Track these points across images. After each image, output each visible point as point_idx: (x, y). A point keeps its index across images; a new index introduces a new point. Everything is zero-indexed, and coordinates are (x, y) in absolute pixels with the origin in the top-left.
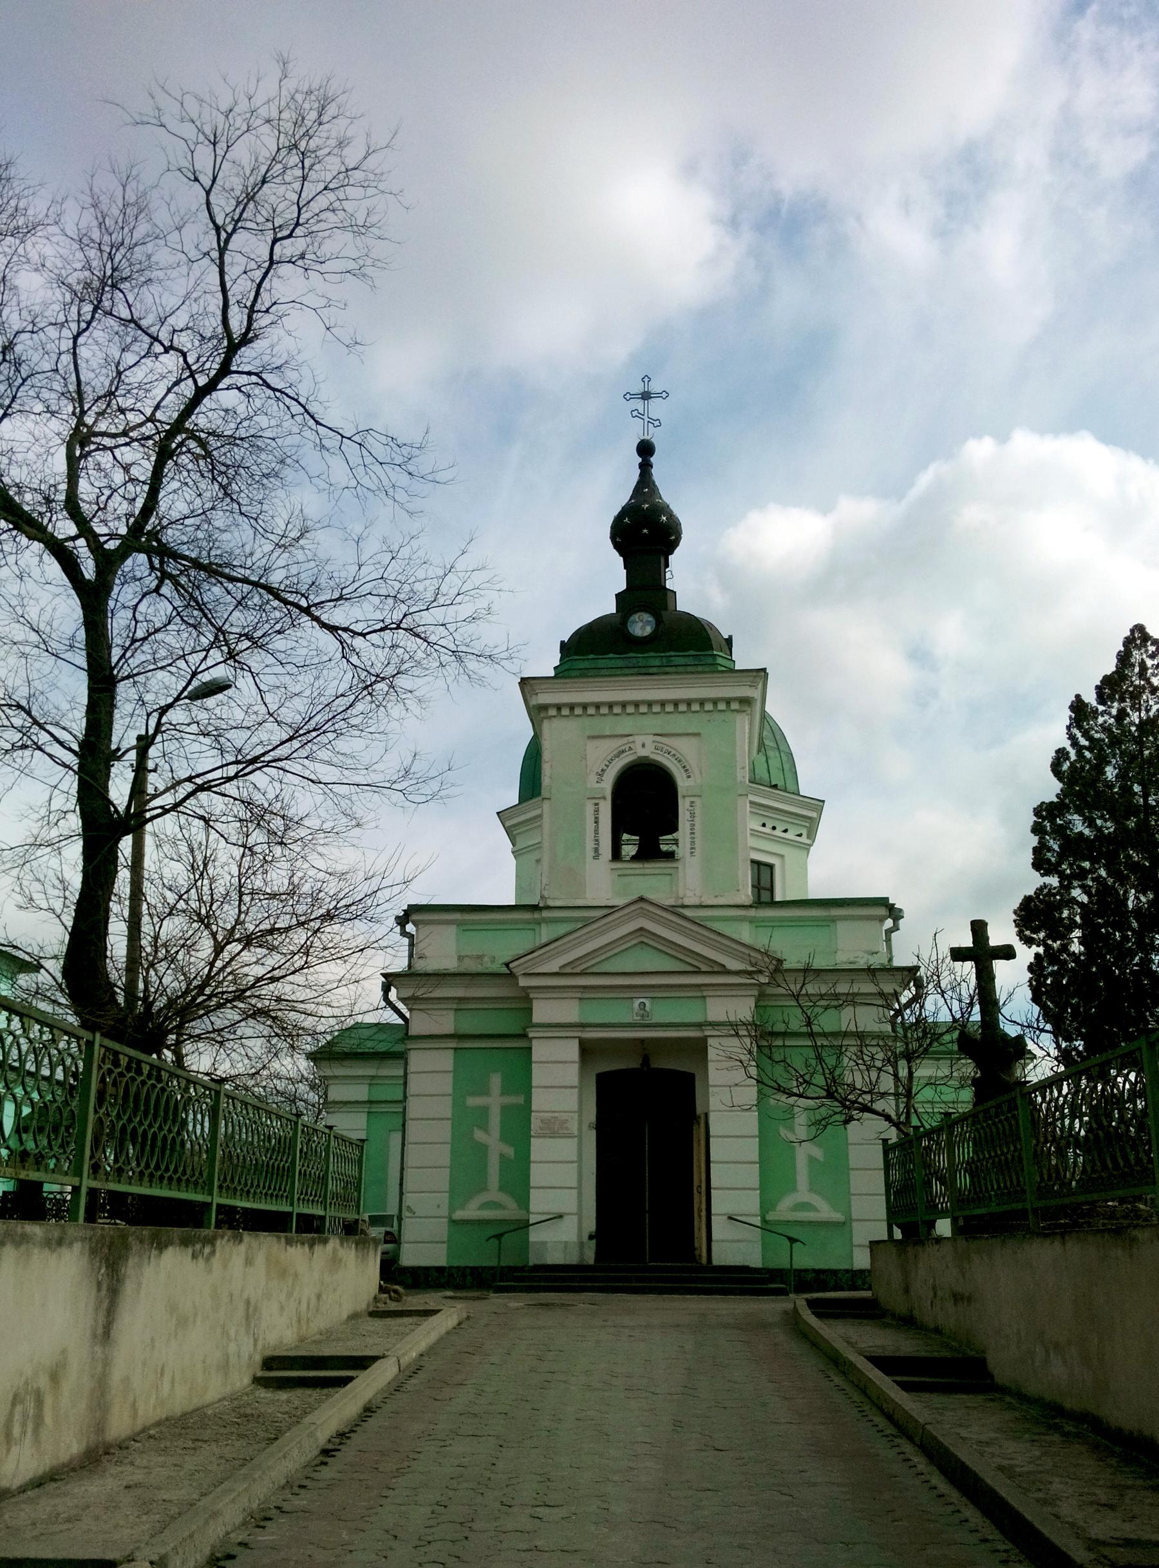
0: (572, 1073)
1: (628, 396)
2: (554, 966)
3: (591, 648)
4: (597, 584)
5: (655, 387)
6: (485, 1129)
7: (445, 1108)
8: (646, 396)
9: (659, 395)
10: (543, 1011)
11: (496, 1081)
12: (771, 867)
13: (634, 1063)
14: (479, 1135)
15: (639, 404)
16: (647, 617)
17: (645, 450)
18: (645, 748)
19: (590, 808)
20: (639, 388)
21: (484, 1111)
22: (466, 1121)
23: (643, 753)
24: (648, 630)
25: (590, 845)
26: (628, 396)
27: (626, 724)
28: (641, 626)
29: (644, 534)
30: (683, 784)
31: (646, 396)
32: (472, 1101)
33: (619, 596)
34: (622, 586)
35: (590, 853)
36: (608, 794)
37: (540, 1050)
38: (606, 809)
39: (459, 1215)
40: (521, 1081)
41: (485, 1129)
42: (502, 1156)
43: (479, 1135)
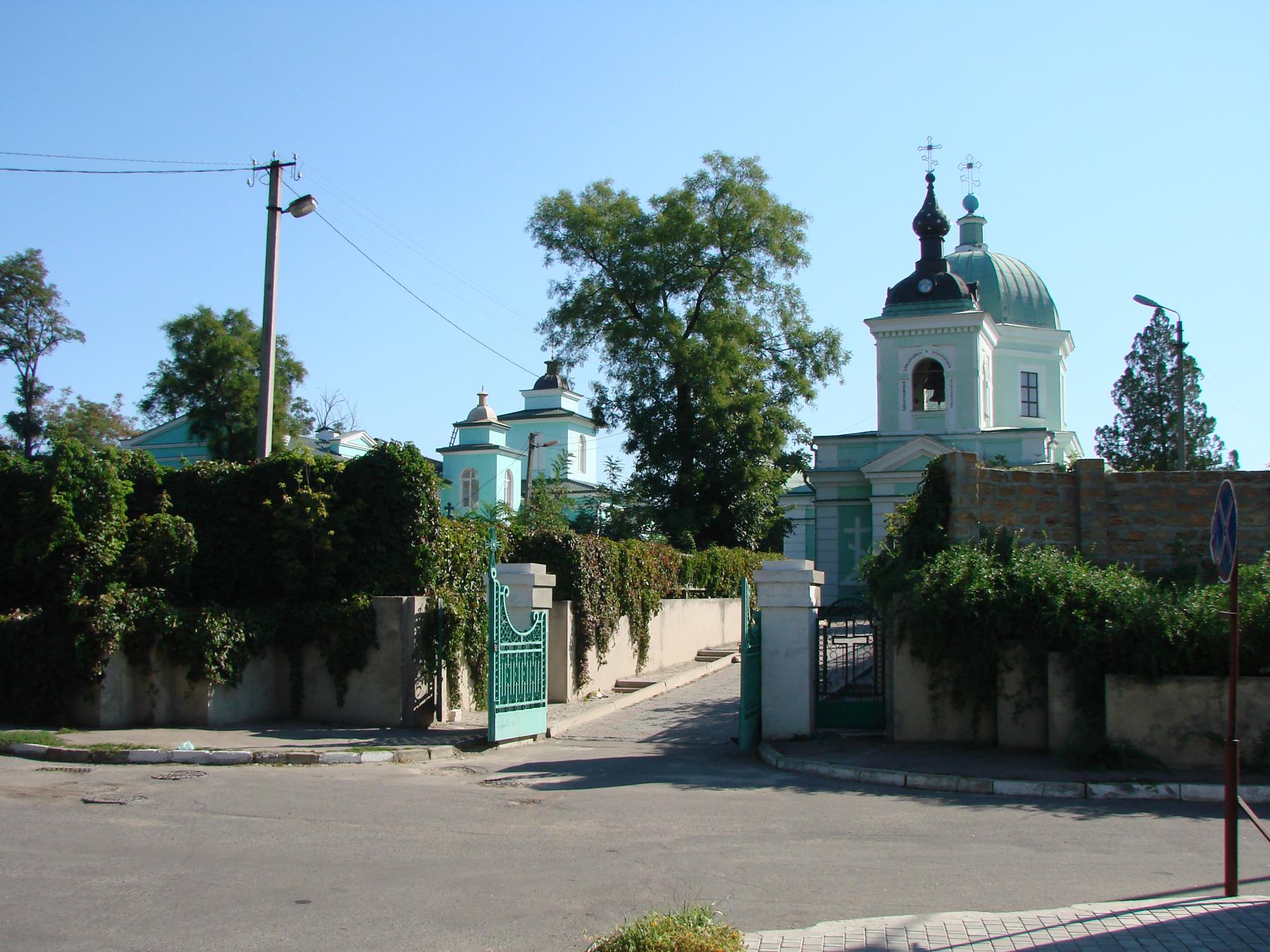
1: (920, 148)
2: (881, 468)
3: (903, 297)
4: (904, 257)
5: (934, 143)
6: (853, 543)
7: (835, 534)
8: (930, 148)
9: (937, 147)
11: (857, 520)
14: (850, 546)
15: (926, 152)
16: (928, 282)
17: (930, 178)
19: (901, 385)
21: (853, 535)
24: (929, 288)
25: (901, 404)
26: (920, 148)
29: (929, 225)
30: (947, 371)
31: (930, 148)
32: (847, 530)
33: (918, 263)
36: (910, 377)
38: (909, 384)
39: (843, 583)
41: (853, 543)
43: (850, 546)
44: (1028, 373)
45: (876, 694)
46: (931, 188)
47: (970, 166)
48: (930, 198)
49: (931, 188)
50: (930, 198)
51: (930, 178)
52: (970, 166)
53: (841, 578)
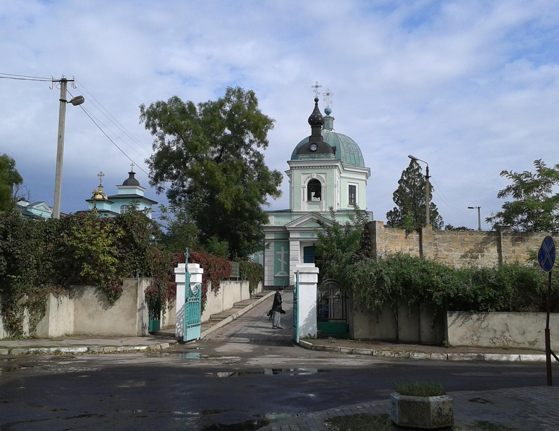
0: (298, 248)
2: (294, 226)
5: (319, 85)
8: (317, 87)
10: (292, 236)
11: (283, 248)
12: (355, 186)
13: (312, 245)
15: (315, 88)
17: (316, 100)
18: (315, 177)
19: (302, 189)
20: (315, 85)
22: (277, 256)
23: (313, 177)
27: (310, 171)
28: (314, 148)
29: (316, 122)
30: (323, 184)
31: (317, 87)
32: (277, 253)
34: (311, 135)
35: (302, 200)
36: (306, 186)
37: (291, 243)
38: (306, 190)
39: (276, 275)
40: (288, 249)
42: (284, 264)
43: (279, 259)
44: (352, 186)
45: (343, 319)
46: (316, 104)
47: (328, 94)
48: (316, 109)
49: (316, 104)
50: (316, 109)
51: (316, 100)
52: (328, 94)
53: (275, 273)
